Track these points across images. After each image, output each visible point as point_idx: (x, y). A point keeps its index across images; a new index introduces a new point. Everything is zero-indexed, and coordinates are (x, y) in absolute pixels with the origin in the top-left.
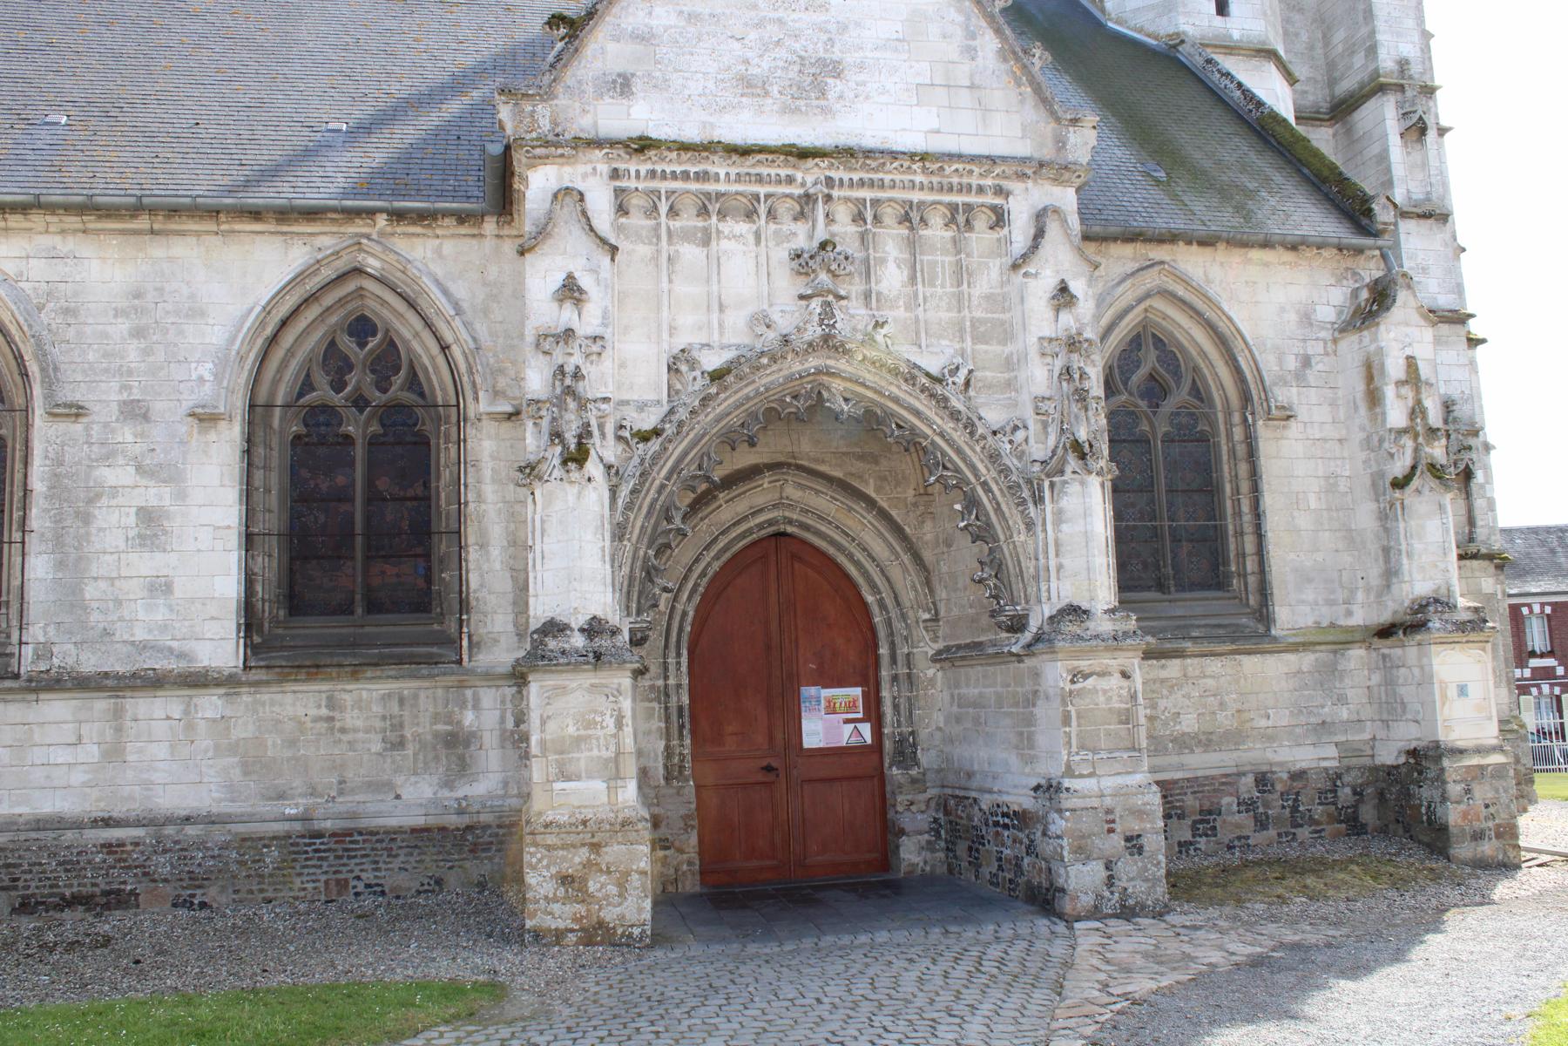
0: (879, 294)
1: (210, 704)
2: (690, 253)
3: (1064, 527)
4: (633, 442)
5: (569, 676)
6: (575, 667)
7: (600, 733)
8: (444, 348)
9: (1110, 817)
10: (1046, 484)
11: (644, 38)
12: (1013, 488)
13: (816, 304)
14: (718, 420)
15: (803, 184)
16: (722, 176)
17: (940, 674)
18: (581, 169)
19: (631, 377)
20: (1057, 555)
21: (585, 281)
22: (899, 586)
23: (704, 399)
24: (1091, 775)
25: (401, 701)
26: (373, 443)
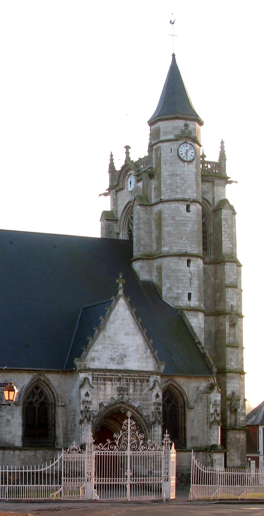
1: (17, 452)
2: (102, 386)
8: (53, 393)
11: (96, 351)
13: (121, 396)
21: (89, 393)
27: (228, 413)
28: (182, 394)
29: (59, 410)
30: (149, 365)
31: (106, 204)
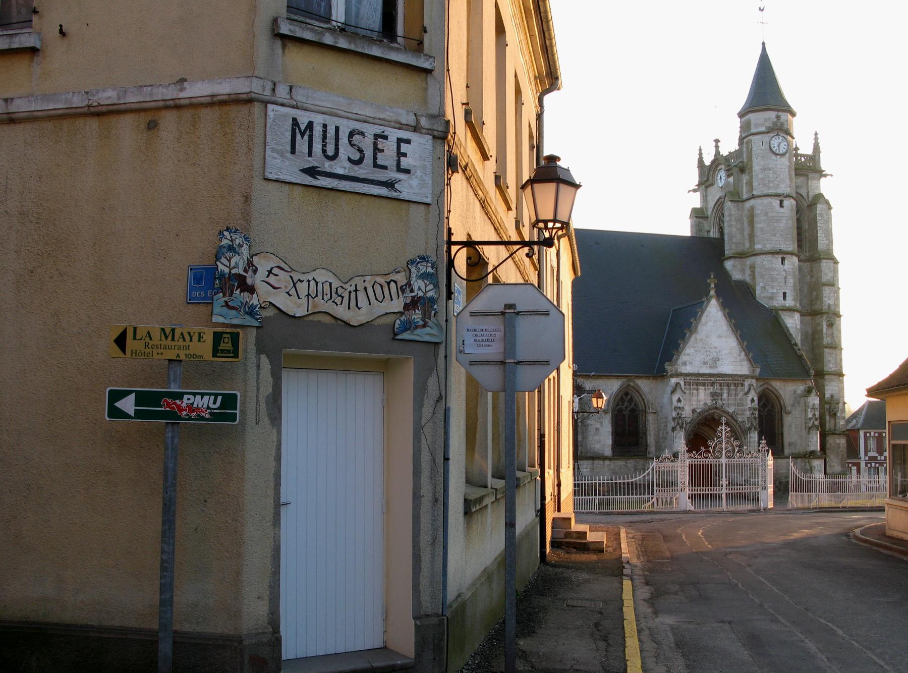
1: (607, 462)
2: (695, 392)
27: (828, 418)
28: (778, 398)
29: (651, 418)
31: (696, 201)
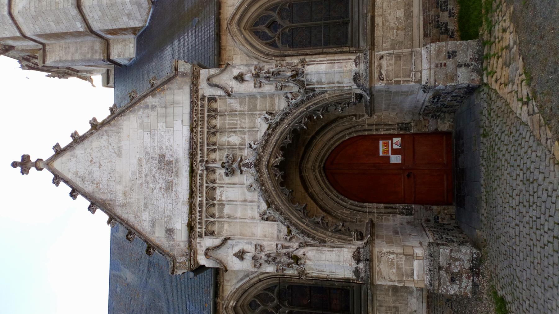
0: (240, 145)
3: (323, 81)
4: (291, 236)
5: (374, 270)
6: (372, 268)
7: (396, 260)
8: (260, 280)
9: (439, 65)
10: (307, 87)
11: (153, 225)
12: (309, 98)
13: (244, 169)
14: (284, 204)
15: (203, 171)
16: (200, 199)
17: (376, 114)
18: (198, 247)
19: (268, 234)
20: (334, 83)
21: (236, 249)
22: (343, 128)
23: (277, 210)
24: (421, 73)
25: (381, 306)
26: (291, 304)
30: (180, 97)
